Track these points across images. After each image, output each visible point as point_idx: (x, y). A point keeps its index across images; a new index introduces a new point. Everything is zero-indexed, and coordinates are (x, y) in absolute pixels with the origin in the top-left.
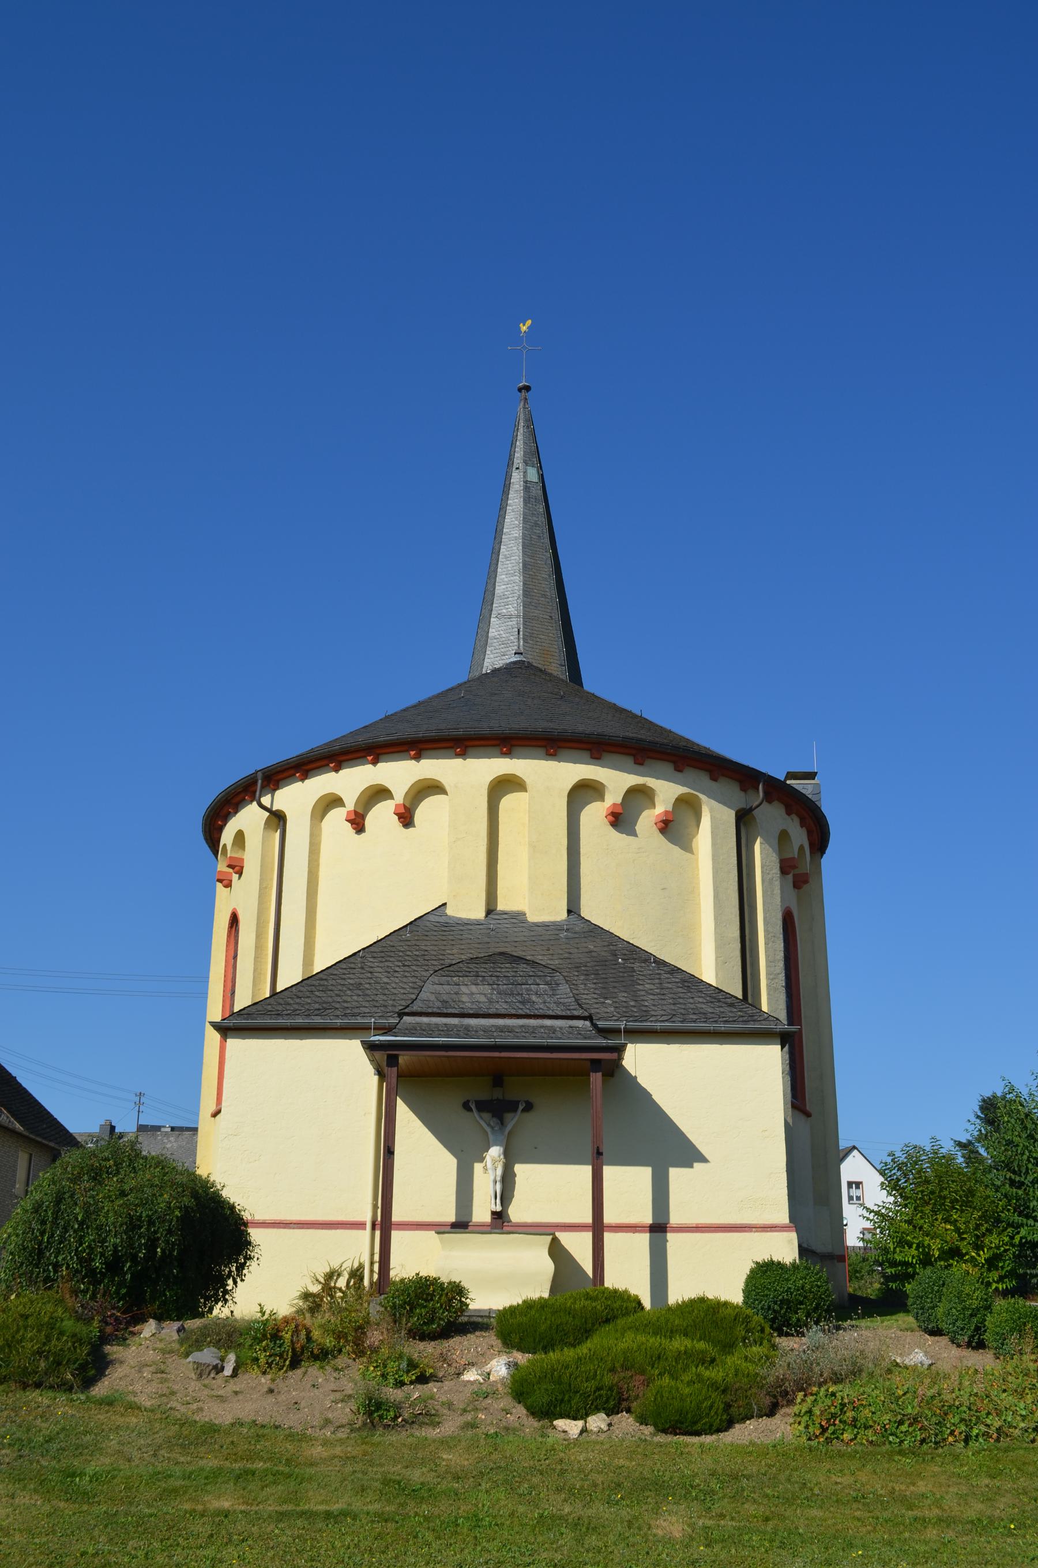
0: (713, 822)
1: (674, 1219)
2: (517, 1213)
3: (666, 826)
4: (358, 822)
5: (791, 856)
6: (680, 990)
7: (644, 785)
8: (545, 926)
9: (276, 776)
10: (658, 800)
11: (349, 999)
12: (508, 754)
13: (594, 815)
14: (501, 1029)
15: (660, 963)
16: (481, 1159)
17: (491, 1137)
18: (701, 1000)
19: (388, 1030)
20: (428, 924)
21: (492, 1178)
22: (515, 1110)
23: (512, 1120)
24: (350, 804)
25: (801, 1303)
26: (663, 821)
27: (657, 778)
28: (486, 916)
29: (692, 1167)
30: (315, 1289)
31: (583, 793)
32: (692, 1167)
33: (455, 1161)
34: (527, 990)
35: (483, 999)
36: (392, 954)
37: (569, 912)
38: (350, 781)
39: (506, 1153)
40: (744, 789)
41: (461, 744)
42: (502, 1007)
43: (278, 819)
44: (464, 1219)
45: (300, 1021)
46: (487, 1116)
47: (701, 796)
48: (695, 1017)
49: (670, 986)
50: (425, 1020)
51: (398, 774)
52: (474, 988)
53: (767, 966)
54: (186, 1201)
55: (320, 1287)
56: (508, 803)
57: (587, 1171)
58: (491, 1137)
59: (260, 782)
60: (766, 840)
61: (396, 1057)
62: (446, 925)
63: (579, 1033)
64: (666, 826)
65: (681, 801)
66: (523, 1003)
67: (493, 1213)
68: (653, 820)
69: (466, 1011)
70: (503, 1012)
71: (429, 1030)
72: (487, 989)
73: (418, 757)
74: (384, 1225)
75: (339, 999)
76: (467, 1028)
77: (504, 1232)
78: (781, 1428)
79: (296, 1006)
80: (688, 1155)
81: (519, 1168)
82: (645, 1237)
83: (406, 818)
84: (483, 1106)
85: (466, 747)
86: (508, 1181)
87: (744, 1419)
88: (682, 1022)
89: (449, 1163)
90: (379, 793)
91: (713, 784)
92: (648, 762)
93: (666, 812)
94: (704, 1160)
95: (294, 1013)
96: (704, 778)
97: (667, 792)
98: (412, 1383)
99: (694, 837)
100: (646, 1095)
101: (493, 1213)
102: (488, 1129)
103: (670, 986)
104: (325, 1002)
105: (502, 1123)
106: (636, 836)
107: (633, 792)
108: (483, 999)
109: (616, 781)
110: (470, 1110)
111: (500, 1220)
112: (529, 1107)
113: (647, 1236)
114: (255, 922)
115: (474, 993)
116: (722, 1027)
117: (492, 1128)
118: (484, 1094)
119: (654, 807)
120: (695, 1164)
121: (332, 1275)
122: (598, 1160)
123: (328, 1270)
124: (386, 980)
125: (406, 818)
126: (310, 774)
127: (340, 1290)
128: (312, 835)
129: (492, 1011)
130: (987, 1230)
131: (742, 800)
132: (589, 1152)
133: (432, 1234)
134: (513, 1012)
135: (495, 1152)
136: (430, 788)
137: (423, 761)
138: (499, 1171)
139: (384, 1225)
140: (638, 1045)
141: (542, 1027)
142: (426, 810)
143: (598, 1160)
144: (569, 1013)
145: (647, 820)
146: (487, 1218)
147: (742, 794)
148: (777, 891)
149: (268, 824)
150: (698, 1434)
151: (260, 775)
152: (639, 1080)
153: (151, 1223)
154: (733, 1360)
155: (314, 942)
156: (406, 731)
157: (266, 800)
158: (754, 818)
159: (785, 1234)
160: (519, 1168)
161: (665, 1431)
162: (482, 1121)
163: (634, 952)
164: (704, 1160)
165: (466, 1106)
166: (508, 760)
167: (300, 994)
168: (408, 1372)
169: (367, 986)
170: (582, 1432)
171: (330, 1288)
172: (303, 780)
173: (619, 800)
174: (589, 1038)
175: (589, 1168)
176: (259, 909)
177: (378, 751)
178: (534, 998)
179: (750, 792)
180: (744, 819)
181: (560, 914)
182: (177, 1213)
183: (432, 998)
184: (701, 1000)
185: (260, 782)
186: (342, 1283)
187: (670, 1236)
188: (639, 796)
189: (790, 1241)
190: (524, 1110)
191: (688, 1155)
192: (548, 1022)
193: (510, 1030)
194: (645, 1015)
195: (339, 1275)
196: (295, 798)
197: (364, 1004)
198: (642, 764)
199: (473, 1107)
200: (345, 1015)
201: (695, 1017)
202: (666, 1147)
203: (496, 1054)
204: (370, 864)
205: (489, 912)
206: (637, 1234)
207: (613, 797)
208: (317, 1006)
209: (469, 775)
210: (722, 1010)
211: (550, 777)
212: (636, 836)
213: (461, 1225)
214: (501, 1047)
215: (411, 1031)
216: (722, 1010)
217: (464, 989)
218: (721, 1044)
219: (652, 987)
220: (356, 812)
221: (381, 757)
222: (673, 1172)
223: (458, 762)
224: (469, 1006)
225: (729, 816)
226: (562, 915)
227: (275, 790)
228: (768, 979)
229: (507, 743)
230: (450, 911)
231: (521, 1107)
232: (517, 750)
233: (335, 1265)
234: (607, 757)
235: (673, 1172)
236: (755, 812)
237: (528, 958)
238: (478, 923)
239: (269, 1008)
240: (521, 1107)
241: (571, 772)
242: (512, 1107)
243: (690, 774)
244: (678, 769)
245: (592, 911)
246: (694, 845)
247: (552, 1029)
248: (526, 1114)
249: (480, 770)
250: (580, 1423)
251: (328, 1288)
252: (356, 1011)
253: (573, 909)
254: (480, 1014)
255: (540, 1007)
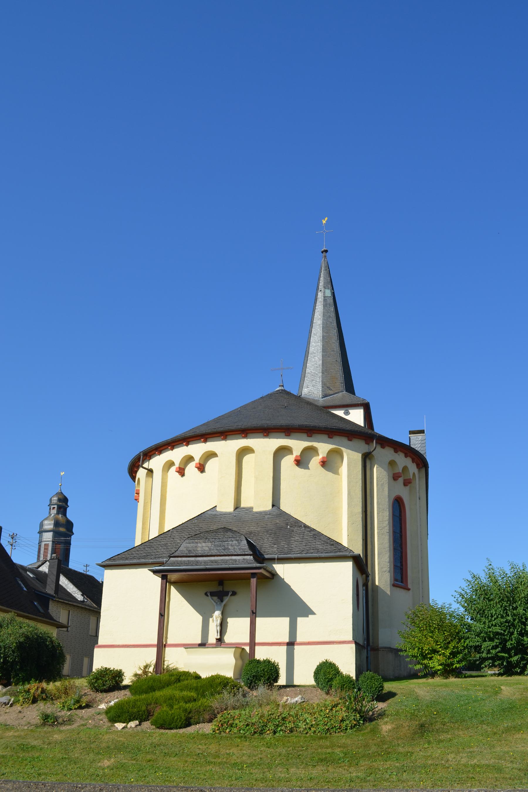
0: (350, 459)
1: (299, 639)
2: (228, 638)
3: (324, 463)
4: (181, 472)
5: (398, 472)
6: (311, 539)
7: (312, 446)
8: (260, 513)
9: (148, 454)
10: (320, 452)
11: (159, 551)
12: (246, 437)
13: (288, 462)
14: (212, 561)
15: (306, 527)
16: (212, 617)
17: (216, 607)
18: (319, 543)
19: (162, 564)
20: (207, 515)
21: (216, 624)
22: (227, 595)
23: (226, 599)
24: (177, 465)
25: (262, 677)
26: (322, 462)
27: (319, 442)
28: (234, 510)
29: (308, 617)
30: (140, 672)
31: (280, 453)
32: (308, 617)
33: (201, 617)
34: (227, 544)
35: (207, 549)
36: (186, 530)
37: (273, 506)
38: (176, 455)
39: (222, 614)
40: (367, 443)
41: (224, 434)
42: (214, 552)
43: (150, 471)
44: (205, 642)
45: (135, 561)
46: (215, 598)
47: (342, 448)
48: (312, 551)
49: (307, 537)
50: (180, 559)
51: (197, 450)
52: (204, 544)
53: (378, 524)
54: (22, 640)
55: (142, 671)
56: (247, 459)
57: (248, 620)
58: (216, 607)
59: (142, 457)
60: (380, 465)
61: (166, 576)
62: (215, 515)
63: (247, 561)
64: (324, 463)
65: (331, 452)
66: (224, 550)
67: (217, 639)
68: (318, 461)
69: (197, 555)
70: (214, 554)
71: (180, 563)
72: (209, 544)
73: (205, 441)
74: (161, 646)
75: (155, 551)
76: (197, 562)
77: (201, 646)
78: (207, 728)
79: (135, 555)
80: (307, 611)
81: (230, 620)
82: (285, 648)
83: (201, 468)
84: (213, 594)
85: (247, 433)
86: (223, 627)
87: (196, 723)
88: (306, 554)
89: (198, 618)
90: (190, 459)
91: (350, 443)
92: (314, 435)
93: (323, 458)
94: (314, 613)
95: (134, 558)
96: (345, 440)
97: (323, 448)
98: (75, 709)
99: (340, 467)
100: (288, 586)
101: (217, 639)
102: (215, 604)
103: (307, 537)
104: (148, 553)
105: (222, 601)
106: (309, 469)
107: (306, 450)
108: (207, 549)
109: (297, 445)
110: (207, 596)
111: (220, 641)
112: (234, 594)
113: (286, 647)
114: (142, 518)
115: (203, 546)
116: (323, 555)
117: (217, 603)
118: (215, 588)
119: (318, 455)
120: (310, 616)
121: (146, 667)
122: (254, 615)
123: (145, 665)
124: (178, 541)
125: (201, 468)
126: (162, 452)
127: (150, 672)
128: (163, 479)
129: (210, 554)
130: (451, 640)
131: (366, 448)
132: (249, 612)
133: (182, 649)
134: (219, 554)
135: (217, 614)
136: (212, 455)
137: (208, 443)
138: (219, 622)
139: (161, 646)
140: (285, 565)
141: (231, 560)
142: (210, 465)
143: (254, 615)
144: (243, 553)
145: (315, 462)
146: (214, 641)
147: (367, 446)
148: (386, 489)
149: (147, 474)
150: (171, 729)
151: (142, 454)
152: (285, 580)
153: (5, 648)
154: (203, 701)
155: (164, 525)
156: (219, 427)
157: (146, 465)
158: (373, 456)
159: (349, 645)
160: (230, 620)
161: (158, 728)
162: (210, 601)
163: (297, 523)
164: (314, 613)
165: (206, 594)
166: (245, 440)
167: (139, 550)
168: (74, 704)
169: (169, 545)
170: (123, 728)
171: (146, 672)
172: (159, 455)
173: (299, 454)
174: (250, 564)
175: (249, 619)
176: (144, 512)
177: (188, 440)
178: (230, 547)
179: (371, 444)
180: (367, 458)
181: (267, 506)
182: (14, 644)
183: (185, 549)
184: (319, 543)
185: (142, 457)
186: (151, 669)
187: (296, 647)
188: (312, 450)
189: (352, 648)
190: (231, 595)
191: (307, 611)
192: (234, 558)
193: (216, 562)
194: (290, 551)
195: (150, 667)
196: (156, 463)
197: (165, 553)
198: (311, 436)
199: (209, 594)
200: (155, 558)
201: (312, 551)
202: (295, 608)
203: (208, 573)
204: (185, 491)
205: (237, 507)
206: (281, 647)
207: (297, 452)
208: (144, 554)
209: (227, 448)
210: (327, 547)
211: (265, 446)
212: (309, 469)
213: (203, 645)
214: (230, 567)
215: (172, 564)
216: (327, 547)
217: (199, 545)
218: (299, 563)
219: (299, 538)
220: (200, 464)
221: (208, 439)
222: (299, 620)
223: (223, 442)
224: (200, 552)
225: (358, 457)
226: (269, 507)
227: (149, 460)
228: (378, 529)
229: (245, 432)
230: (218, 509)
231: (230, 594)
232: (249, 435)
233: (148, 662)
234: (293, 435)
235: (299, 620)
236: (373, 453)
237: (234, 529)
238: (230, 513)
239: (124, 556)
240: (230, 594)
241: (275, 443)
242: (226, 594)
243: (337, 439)
244: (330, 437)
245: (287, 506)
246: (340, 471)
247: (235, 560)
248: (233, 597)
249: (236, 444)
250: (124, 725)
251: (145, 672)
252: (160, 556)
253: (275, 504)
254: (208, 555)
255: (232, 552)
